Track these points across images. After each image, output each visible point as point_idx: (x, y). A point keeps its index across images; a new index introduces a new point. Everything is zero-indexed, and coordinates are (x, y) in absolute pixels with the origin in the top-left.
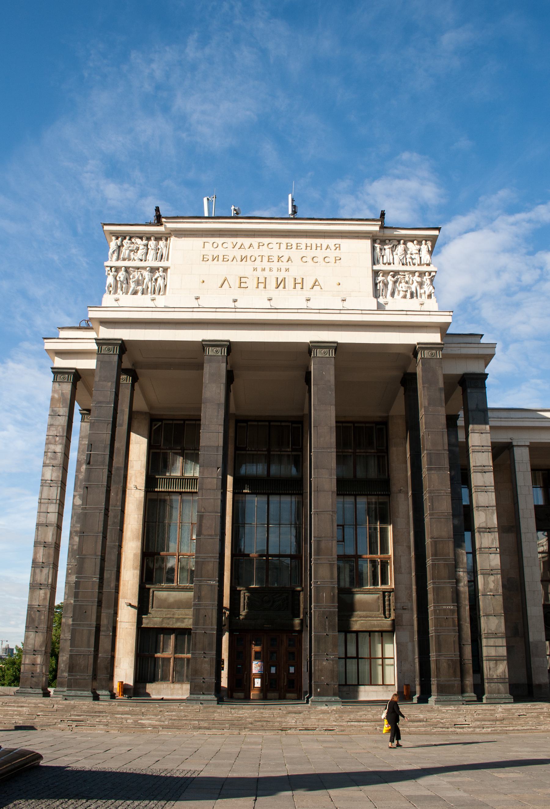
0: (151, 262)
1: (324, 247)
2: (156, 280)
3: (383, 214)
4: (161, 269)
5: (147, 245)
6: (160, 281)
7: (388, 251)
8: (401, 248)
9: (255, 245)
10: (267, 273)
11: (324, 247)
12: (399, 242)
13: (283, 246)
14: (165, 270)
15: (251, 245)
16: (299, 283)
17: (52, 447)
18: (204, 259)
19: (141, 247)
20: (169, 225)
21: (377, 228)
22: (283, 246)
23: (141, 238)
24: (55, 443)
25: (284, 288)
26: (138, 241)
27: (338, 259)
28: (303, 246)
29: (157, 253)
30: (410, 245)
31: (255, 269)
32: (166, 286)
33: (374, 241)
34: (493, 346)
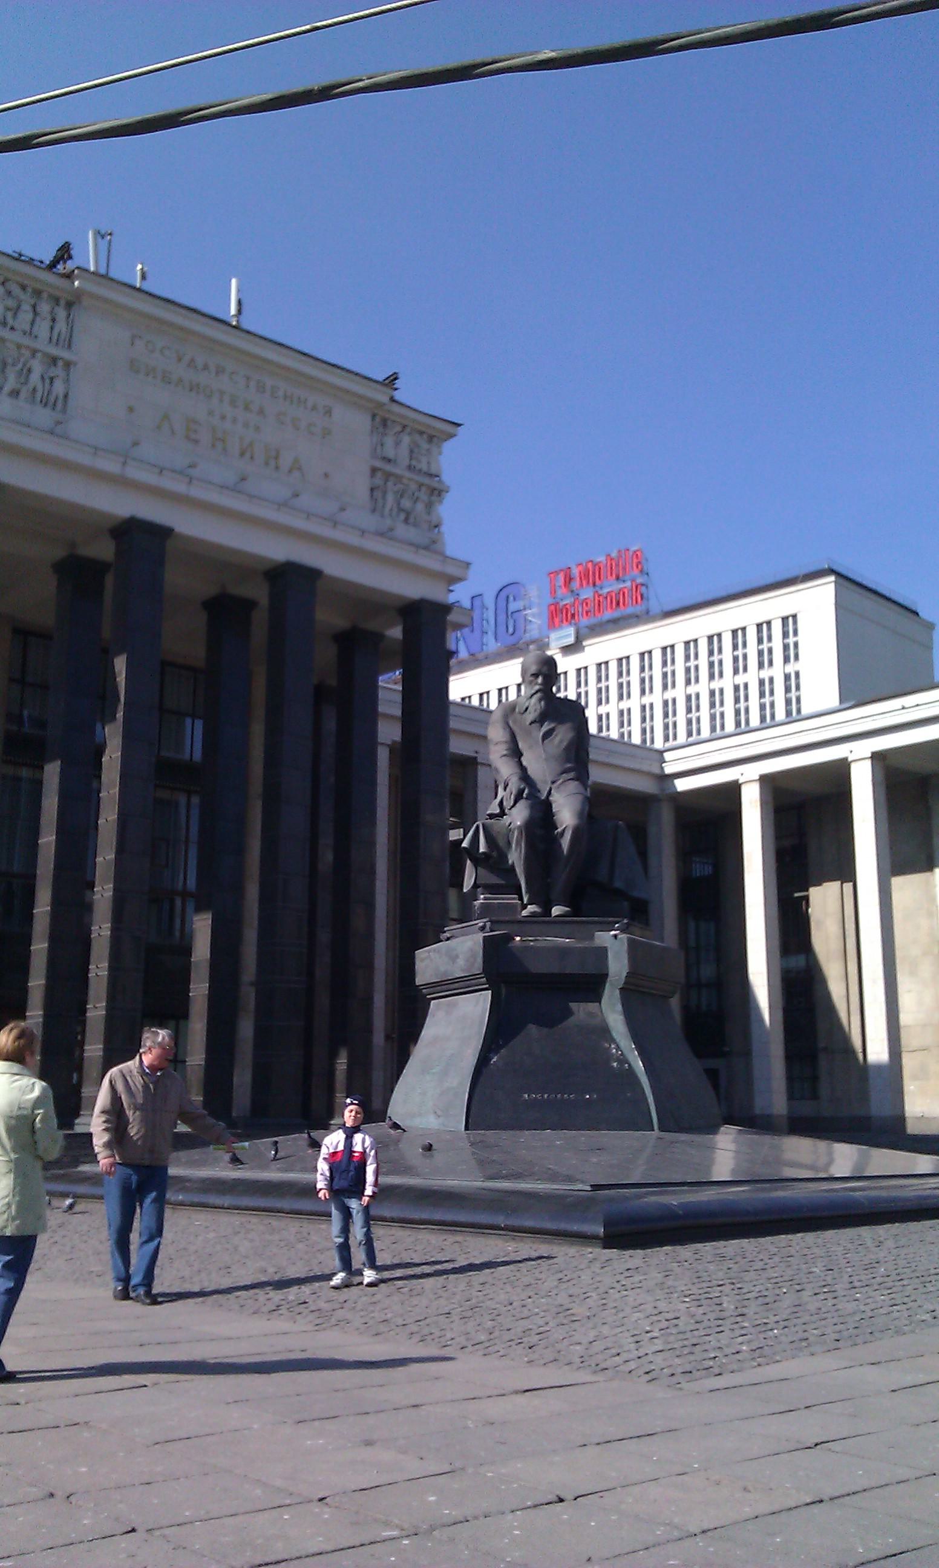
0: (42, 344)
1: (310, 404)
2: (52, 379)
3: (394, 377)
4: (60, 363)
5: (34, 307)
6: (59, 388)
7: (389, 441)
8: (406, 439)
11: (310, 404)
12: (404, 427)
13: (252, 384)
14: (68, 365)
15: (206, 367)
16: (273, 457)
18: (134, 366)
19: (26, 307)
21: (385, 399)
22: (252, 384)
23: (24, 288)
25: (252, 458)
26: (17, 291)
27: (326, 433)
28: (281, 393)
29: (52, 328)
30: (417, 437)
31: (211, 413)
32: (66, 396)
33: (374, 416)
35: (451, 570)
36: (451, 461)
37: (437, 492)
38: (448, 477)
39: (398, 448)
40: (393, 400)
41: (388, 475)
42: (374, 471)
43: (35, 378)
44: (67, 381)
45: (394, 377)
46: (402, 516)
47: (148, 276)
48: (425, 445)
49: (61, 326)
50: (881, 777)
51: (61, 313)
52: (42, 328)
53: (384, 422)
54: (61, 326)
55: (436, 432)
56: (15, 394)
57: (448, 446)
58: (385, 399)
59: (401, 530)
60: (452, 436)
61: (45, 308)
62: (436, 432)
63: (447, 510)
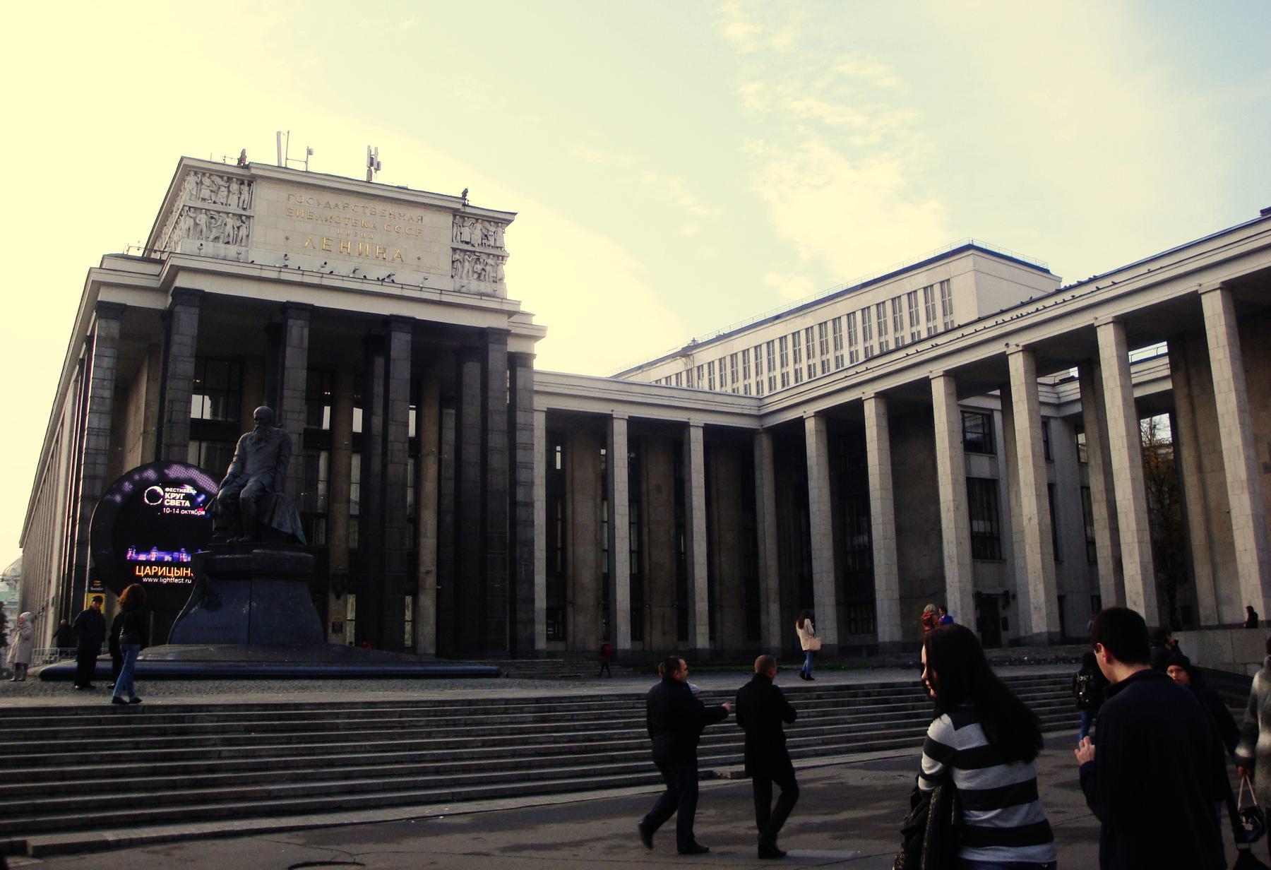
0: (233, 208)
3: (465, 193)
6: (243, 232)
8: (479, 226)
9: (341, 206)
10: (351, 237)
13: (368, 211)
14: (248, 217)
17: (100, 392)
20: (254, 171)
22: (368, 211)
23: (222, 177)
24: (103, 388)
26: (218, 180)
28: (387, 214)
30: (487, 224)
33: (455, 216)
34: (542, 330)
35: (506, 307)
36: (511, 238)
37: (501, 258)
38: (508, 248)
39: (473, 233)
40: (464, 205)
41: (466, 251)
42: (454, 250)
43: (229, 229)
44: (248, 228)
45: (465, 193)
46: (476, 276)
47: (315, 152)
48: (493, 229)
49: (245, 196)
50: (882, 410)
51: (245, 188)
52: (233, 200)
53: (463, 217)
54: (245, 196)
55: (501, 220)
56: (217, 238)
57: (509, 229)
58: (460, 206)
59: (475, 286)
60: (510, 222)
61: (234, 187)
62: (501, 220)
63: (509, 270)
